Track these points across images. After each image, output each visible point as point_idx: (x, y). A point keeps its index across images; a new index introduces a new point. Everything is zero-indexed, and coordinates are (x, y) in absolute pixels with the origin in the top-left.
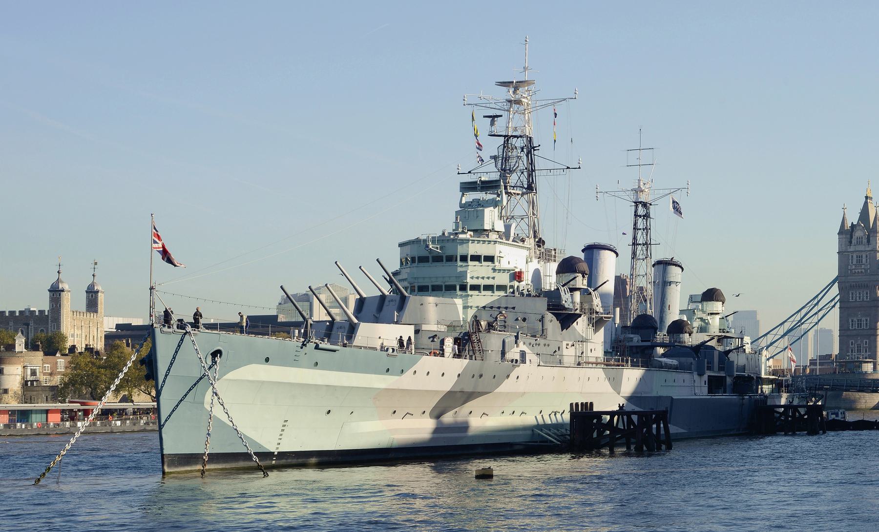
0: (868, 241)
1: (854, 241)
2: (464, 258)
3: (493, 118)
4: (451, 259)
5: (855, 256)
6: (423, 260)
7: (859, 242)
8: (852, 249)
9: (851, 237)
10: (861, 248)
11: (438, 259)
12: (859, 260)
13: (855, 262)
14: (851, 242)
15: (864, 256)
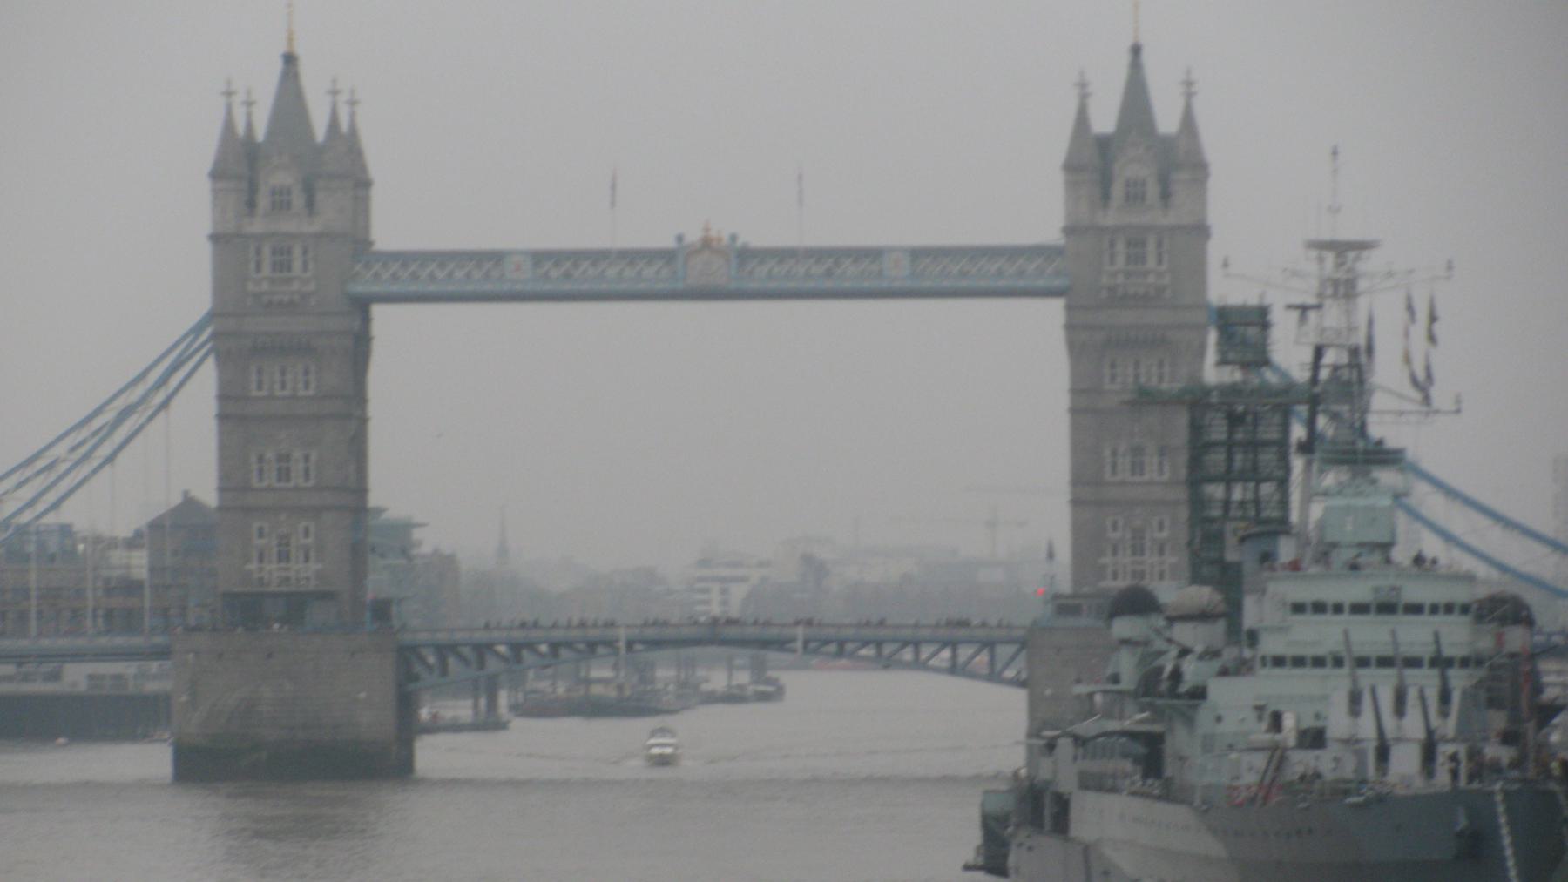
0: (310, 204)
1: (263, 202)
2: (1434, 609)
3: (1304, 309)
4: (1415, 609)
5: (267, 251)
6: (1359, 609)
7: (281, 203)
8: (257, 226)
9: (253, 190)
10: (288, 226)
11: (1387, 608)
12: (282, 265)
13: (266, 270)
14: (251, 204)
15: (297, 252)
